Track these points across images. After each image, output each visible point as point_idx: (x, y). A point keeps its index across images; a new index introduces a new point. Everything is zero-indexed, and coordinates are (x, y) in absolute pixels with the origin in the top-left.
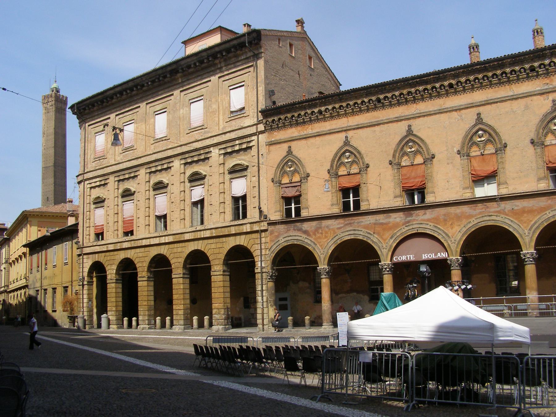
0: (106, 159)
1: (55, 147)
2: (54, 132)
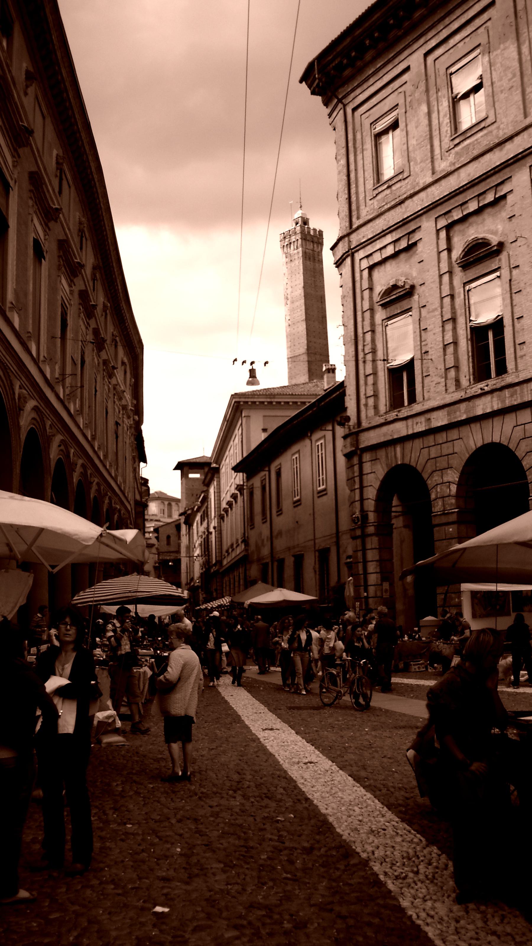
0: (407, 181)
1: (308, 319)
2: (303, 294)
